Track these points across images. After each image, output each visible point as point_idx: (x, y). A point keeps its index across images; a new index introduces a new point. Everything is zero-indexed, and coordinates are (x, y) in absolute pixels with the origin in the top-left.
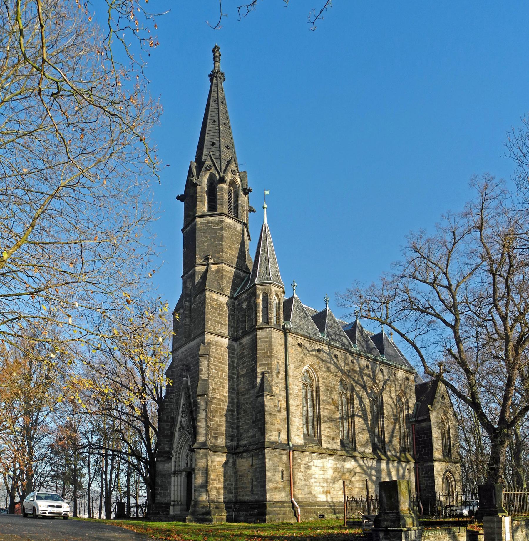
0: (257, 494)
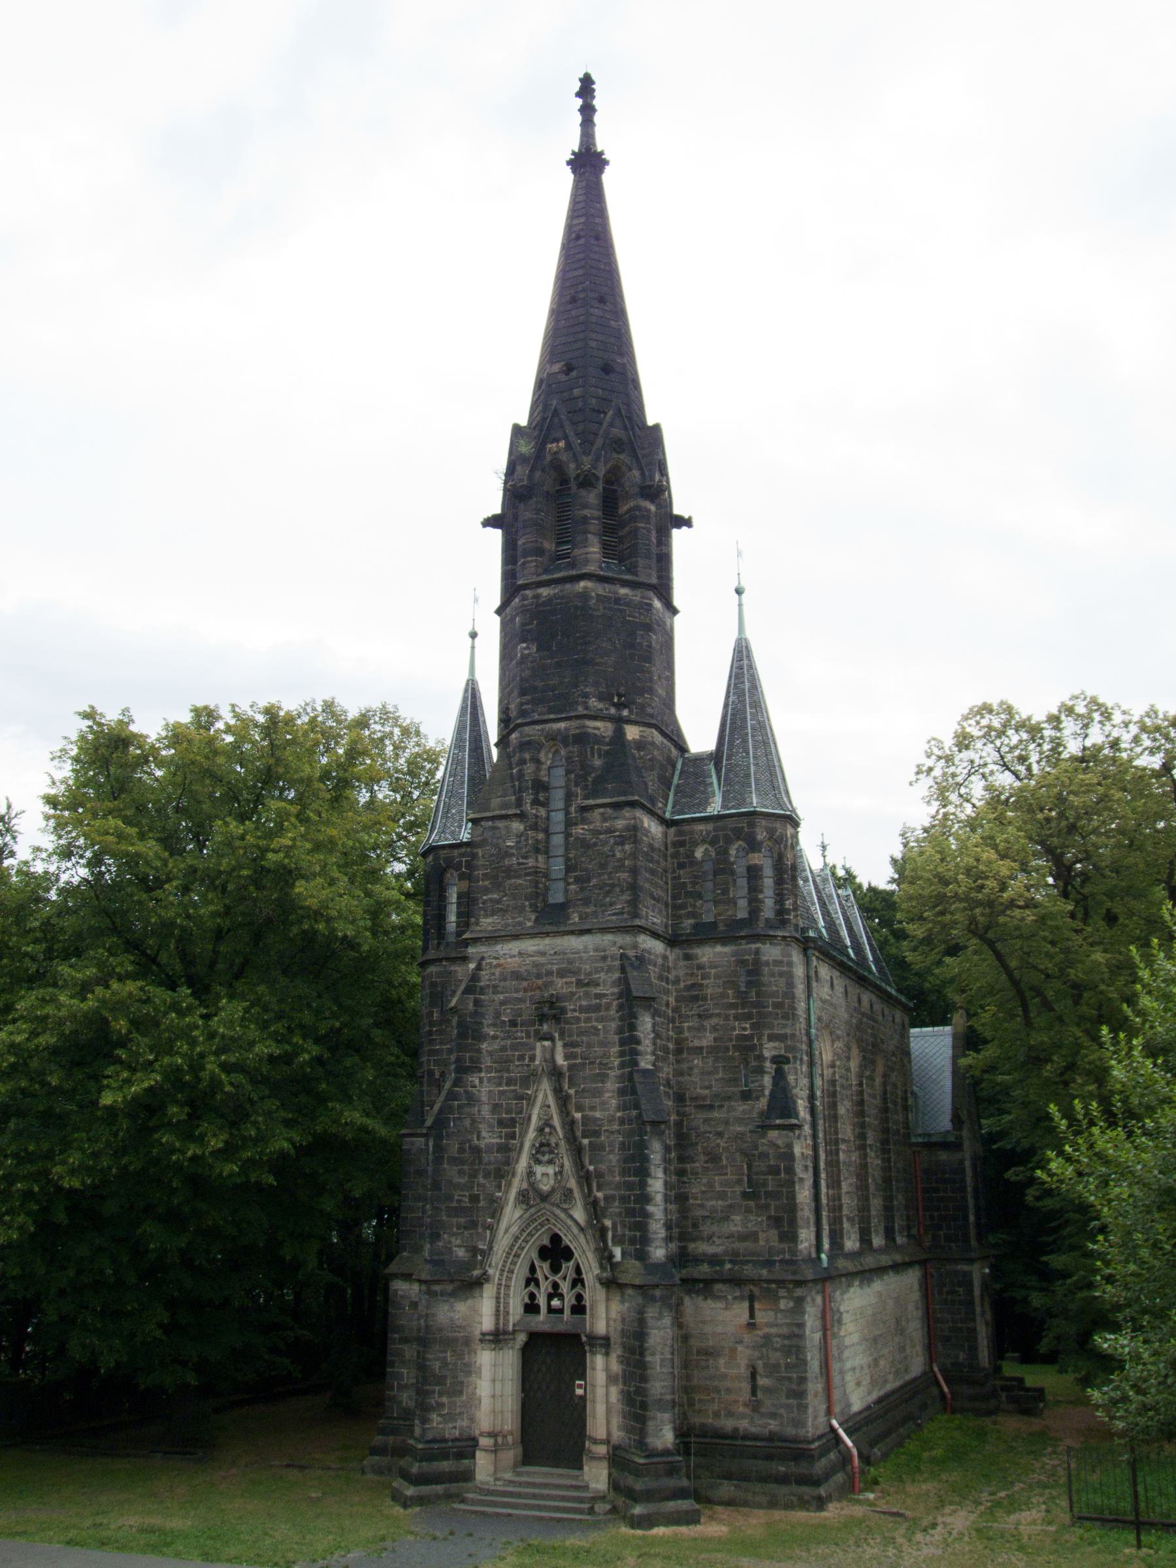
0: (773, 1415)
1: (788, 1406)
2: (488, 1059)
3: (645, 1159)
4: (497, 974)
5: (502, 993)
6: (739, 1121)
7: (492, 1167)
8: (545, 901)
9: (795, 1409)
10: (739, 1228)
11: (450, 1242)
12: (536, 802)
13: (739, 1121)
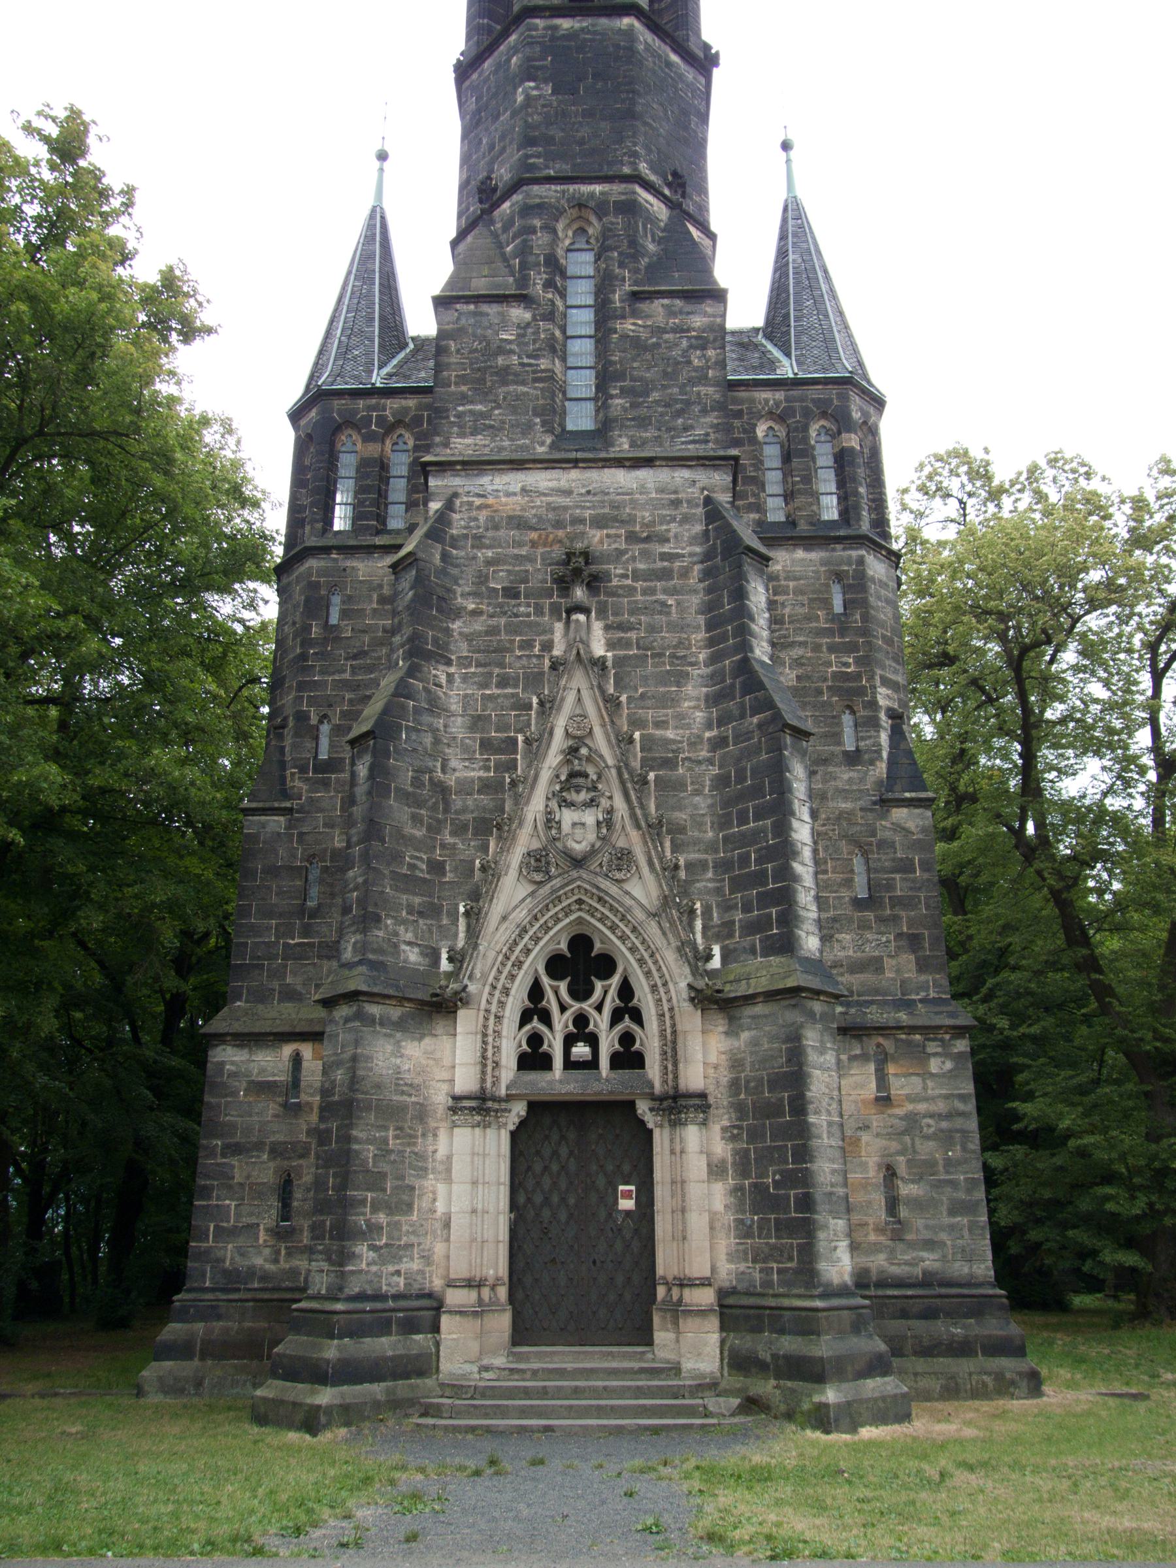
0: (930, 1245)
1: (952, 1228)
2: (464, 646)
3: (782, 789)
4: (482, 519)
5: (488, 547)
6: (844, 794)
7: (470, 816)
8: (562, 425)
9: (966, 1233)
10: (851, 953)
11: (396, 934)
12: (549, 284)
13: (844, 794)
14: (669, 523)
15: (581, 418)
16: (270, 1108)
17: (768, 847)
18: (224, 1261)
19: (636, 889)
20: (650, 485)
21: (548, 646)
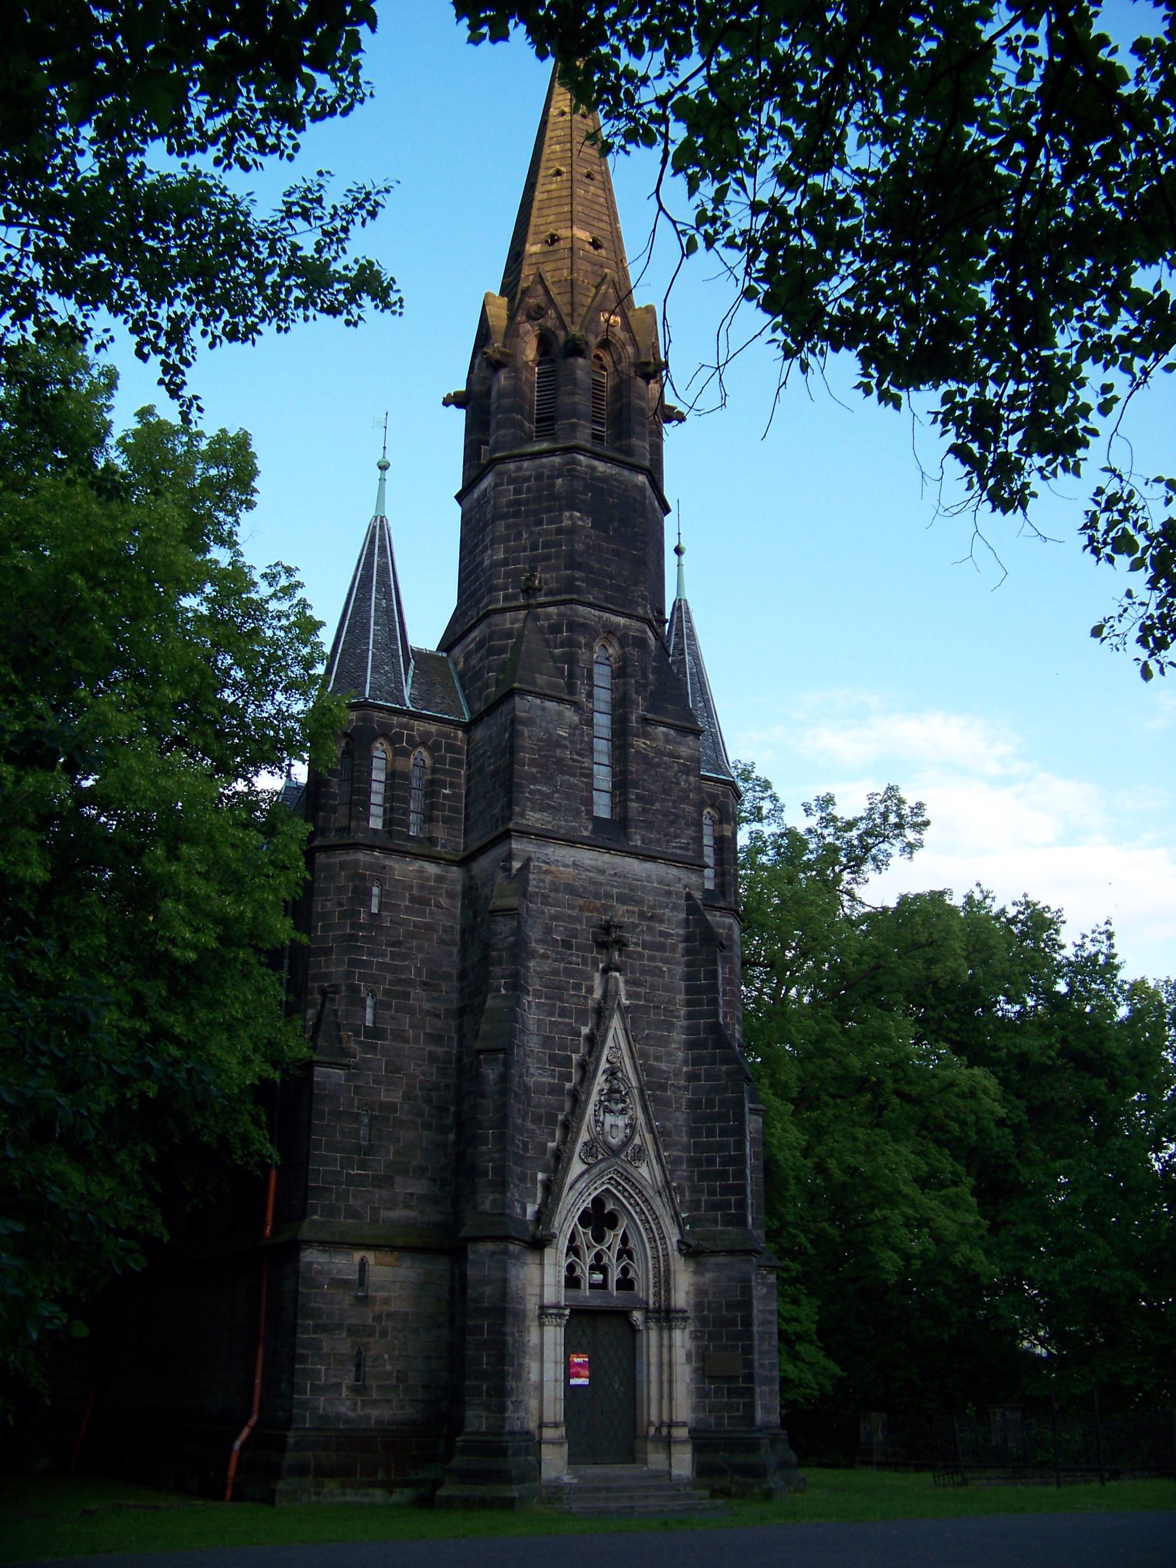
7: (543, 1111)
14: (665, 908)
15: (602, 807)
16: (346, 1299)
17: (730, 1156)
18: (318, 1408)
19: (644, 1171)
20: (654, 877)
21: (590, 990)
